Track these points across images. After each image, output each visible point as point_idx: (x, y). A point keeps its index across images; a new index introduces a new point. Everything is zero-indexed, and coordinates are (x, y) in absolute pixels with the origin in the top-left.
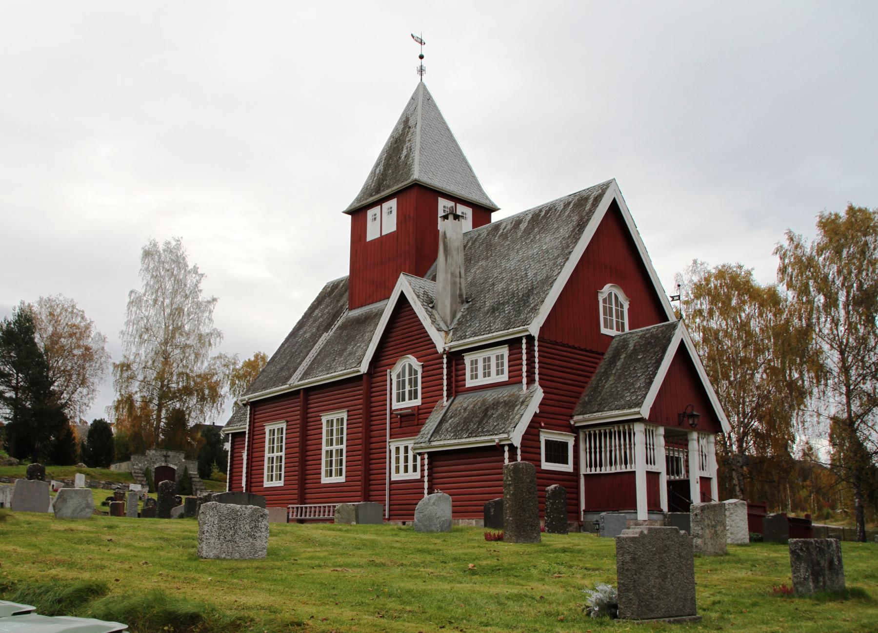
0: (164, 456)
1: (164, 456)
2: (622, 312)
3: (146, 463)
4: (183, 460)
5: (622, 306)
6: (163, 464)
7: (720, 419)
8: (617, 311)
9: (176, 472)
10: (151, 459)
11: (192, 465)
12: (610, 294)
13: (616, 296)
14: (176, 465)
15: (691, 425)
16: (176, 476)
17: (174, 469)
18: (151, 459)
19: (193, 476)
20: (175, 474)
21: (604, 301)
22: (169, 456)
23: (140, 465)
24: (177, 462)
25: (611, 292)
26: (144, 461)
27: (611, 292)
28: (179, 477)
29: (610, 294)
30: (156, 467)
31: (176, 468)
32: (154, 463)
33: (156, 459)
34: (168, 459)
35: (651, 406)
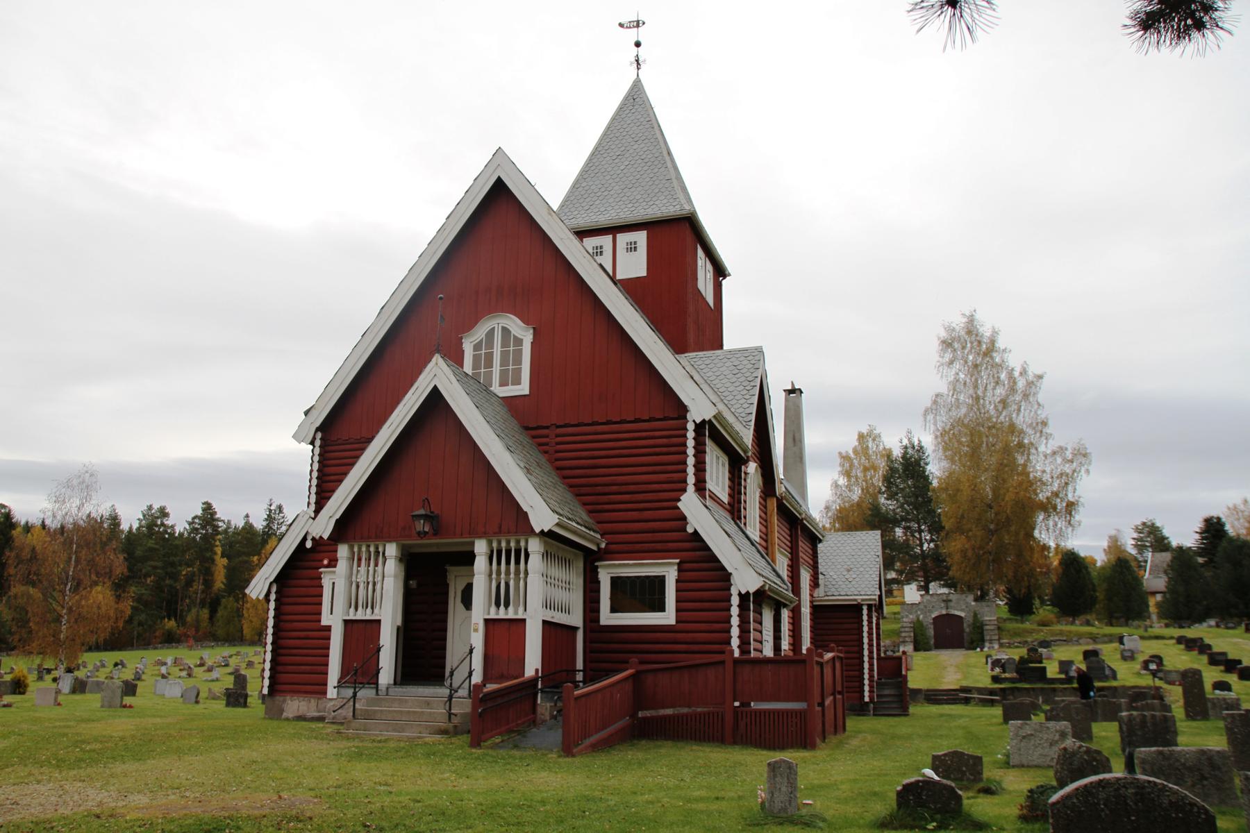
0: (944, 601)
1: (944, 601)
2: (518, 354)
3: (919, 613)
4: (973, 603)
5: (519, 342)
6: (944, 612)
7: (525, 508)
8: (505, 355)
9: (965, 621)
10: (925, 607)
11: (986, 609)
12: (491, 334)
13: (506, 331)
14: (962, 610)
15: (419, 533)
16: (965, 625)
17: (960, 617)
18: (925, 607)
19: (988, 623)
20: (962, 623)
21: (477, 347)
22: (950, 601)
23: (911, 617)
24: (964, 607)
25: (494, 328)
26: (916, 611)
27: (494, 328)
28: (969, 626)
29: (491, 334)
30: (933, 616)
31: (963, 614)
32: (931, 612)
33: (933, 607)
34: (951, 604)
35: (338, 516)
